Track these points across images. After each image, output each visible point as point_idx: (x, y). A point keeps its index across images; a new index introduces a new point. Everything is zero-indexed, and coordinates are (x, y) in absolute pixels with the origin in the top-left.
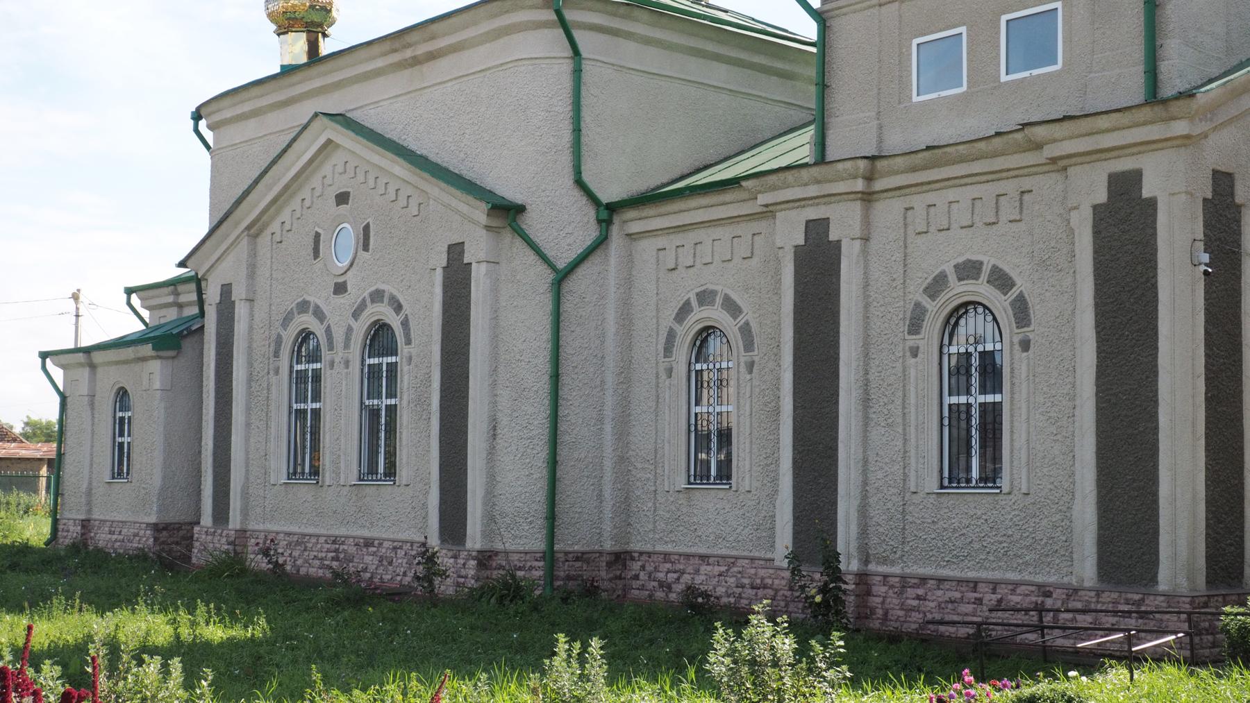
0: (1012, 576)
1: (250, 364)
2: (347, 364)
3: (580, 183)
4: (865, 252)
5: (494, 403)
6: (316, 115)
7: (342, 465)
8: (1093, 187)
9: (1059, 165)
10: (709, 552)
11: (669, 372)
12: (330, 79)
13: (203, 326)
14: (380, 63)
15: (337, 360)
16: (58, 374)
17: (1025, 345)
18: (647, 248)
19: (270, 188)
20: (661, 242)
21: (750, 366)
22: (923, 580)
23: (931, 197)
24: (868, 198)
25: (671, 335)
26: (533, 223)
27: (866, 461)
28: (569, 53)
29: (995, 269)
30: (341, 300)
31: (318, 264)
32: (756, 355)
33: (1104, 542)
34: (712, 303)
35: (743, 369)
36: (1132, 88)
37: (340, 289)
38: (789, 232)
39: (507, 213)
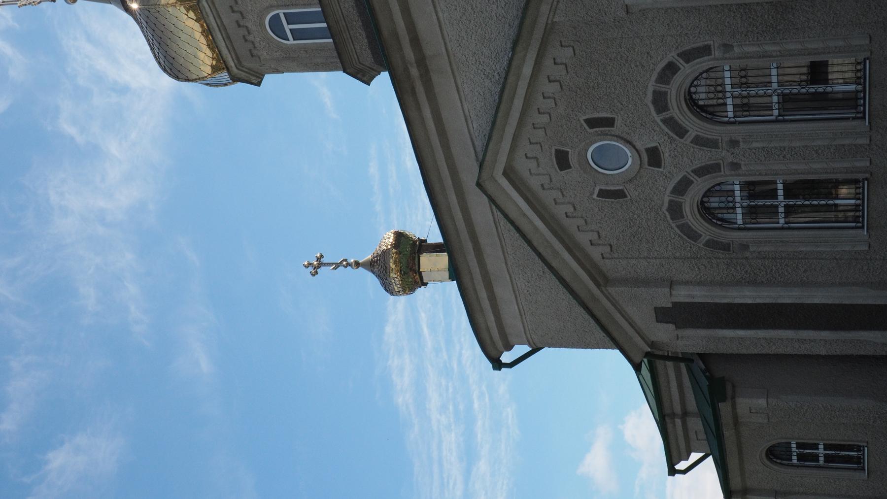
2: (734, 143)
6: (479, 185)
7: (847, 142)
12: (448, 182)
13: (702, 356)
14: (427, 113)
15: (730, 159)
19: (556, 254)
30: (666, 156)
31: (632, 192)
37: (654, 157)
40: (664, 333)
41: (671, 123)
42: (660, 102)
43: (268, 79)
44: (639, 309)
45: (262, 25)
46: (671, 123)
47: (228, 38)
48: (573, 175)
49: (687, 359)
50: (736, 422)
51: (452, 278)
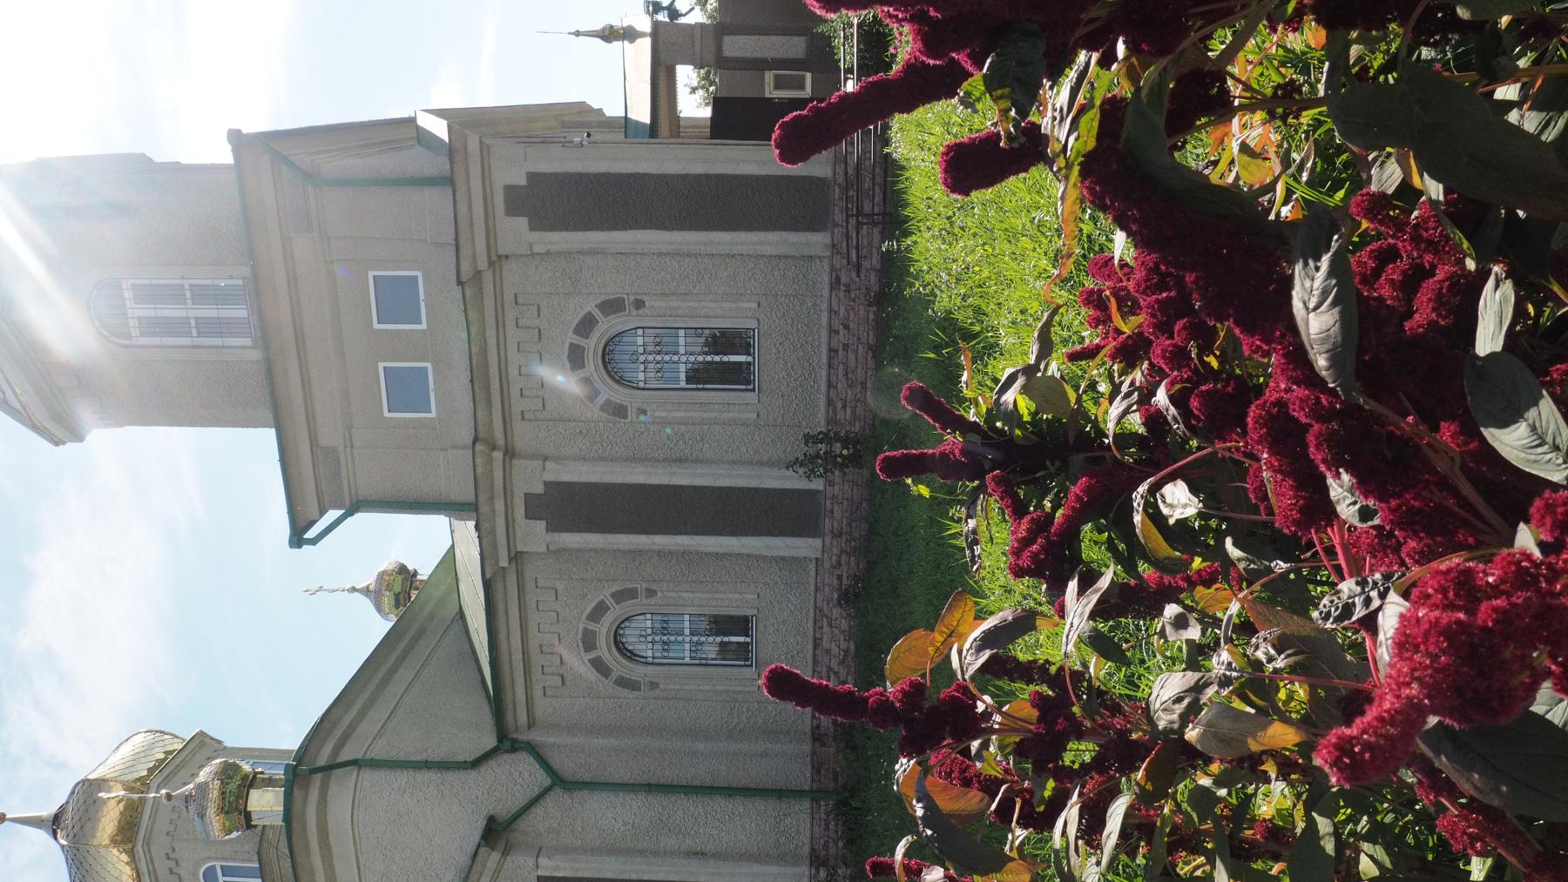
0: (824, 333)
3: (476, 763)
4: (558, 459)
5: (673, 853)
8: (515, 232)
9: (497, 260)
10: (811, 641)
11: (654, 685)
18: (542, 707)
20: (538, 693)
21: (651, 593)
22: (830, 403)
23: (515, 392)
24: (510, 453)
25: (623, 683)
26: (504, 809)
27: (733, 462)
28: (354, 771)
29: (577, 331)
32: (641, 586)
33: (795, 226)
34: (594, 633)
35: (652, 601)
36: (438, 199)
38: (535, 536)
39: (495, 832)
45: (195, 875)
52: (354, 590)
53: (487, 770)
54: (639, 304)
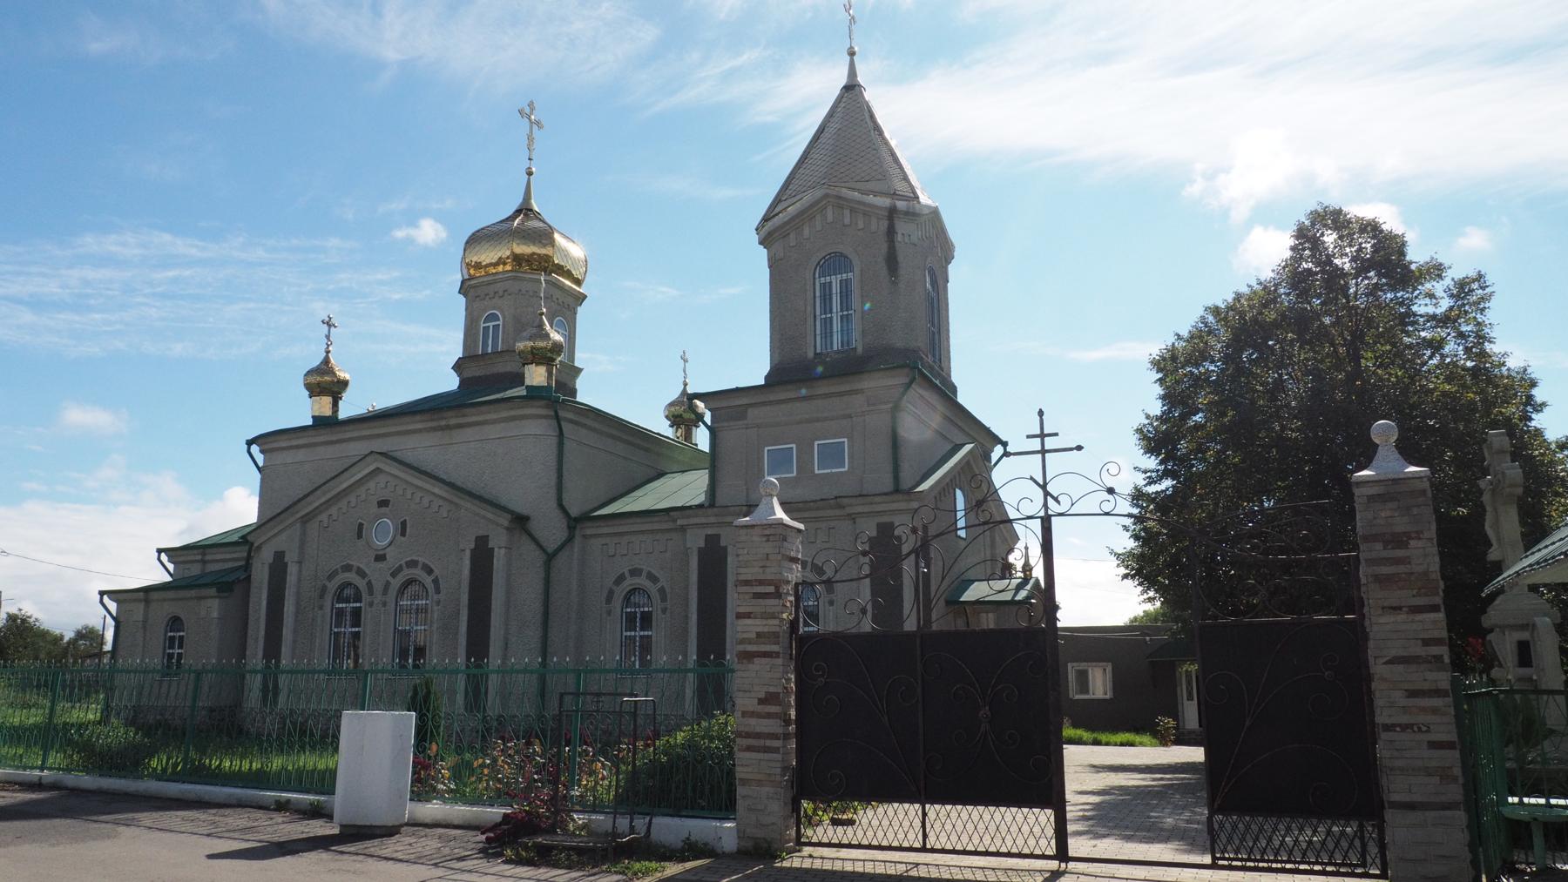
1: (298, 604)
2: (384, 604)
8: (870, 529)
9: (852, 518)
11: (609, 613)
13: (248, 578)
16: (113, 606)
17: (831, 603)
19: (324, 493)
20: (607, 540)
21: (664, 611)
25: (611, 593)
26: (534, 526)
30: (380, 565)
36: (887, 483)
37: (380, 558)
38: (696, 540)
39: (520, 522)
40: (266, 556)
41: (400, 569)
42: (412, 564)
43: (462, 300)
44: (285, 541)
46: (400, 569)
47: (489, 283)
48: (374, 509)
49: (247, 567)
50: (200, 598)
51: (314, 417)
52: (686, 385)
53: (556, 514)
54: (831, 603)
